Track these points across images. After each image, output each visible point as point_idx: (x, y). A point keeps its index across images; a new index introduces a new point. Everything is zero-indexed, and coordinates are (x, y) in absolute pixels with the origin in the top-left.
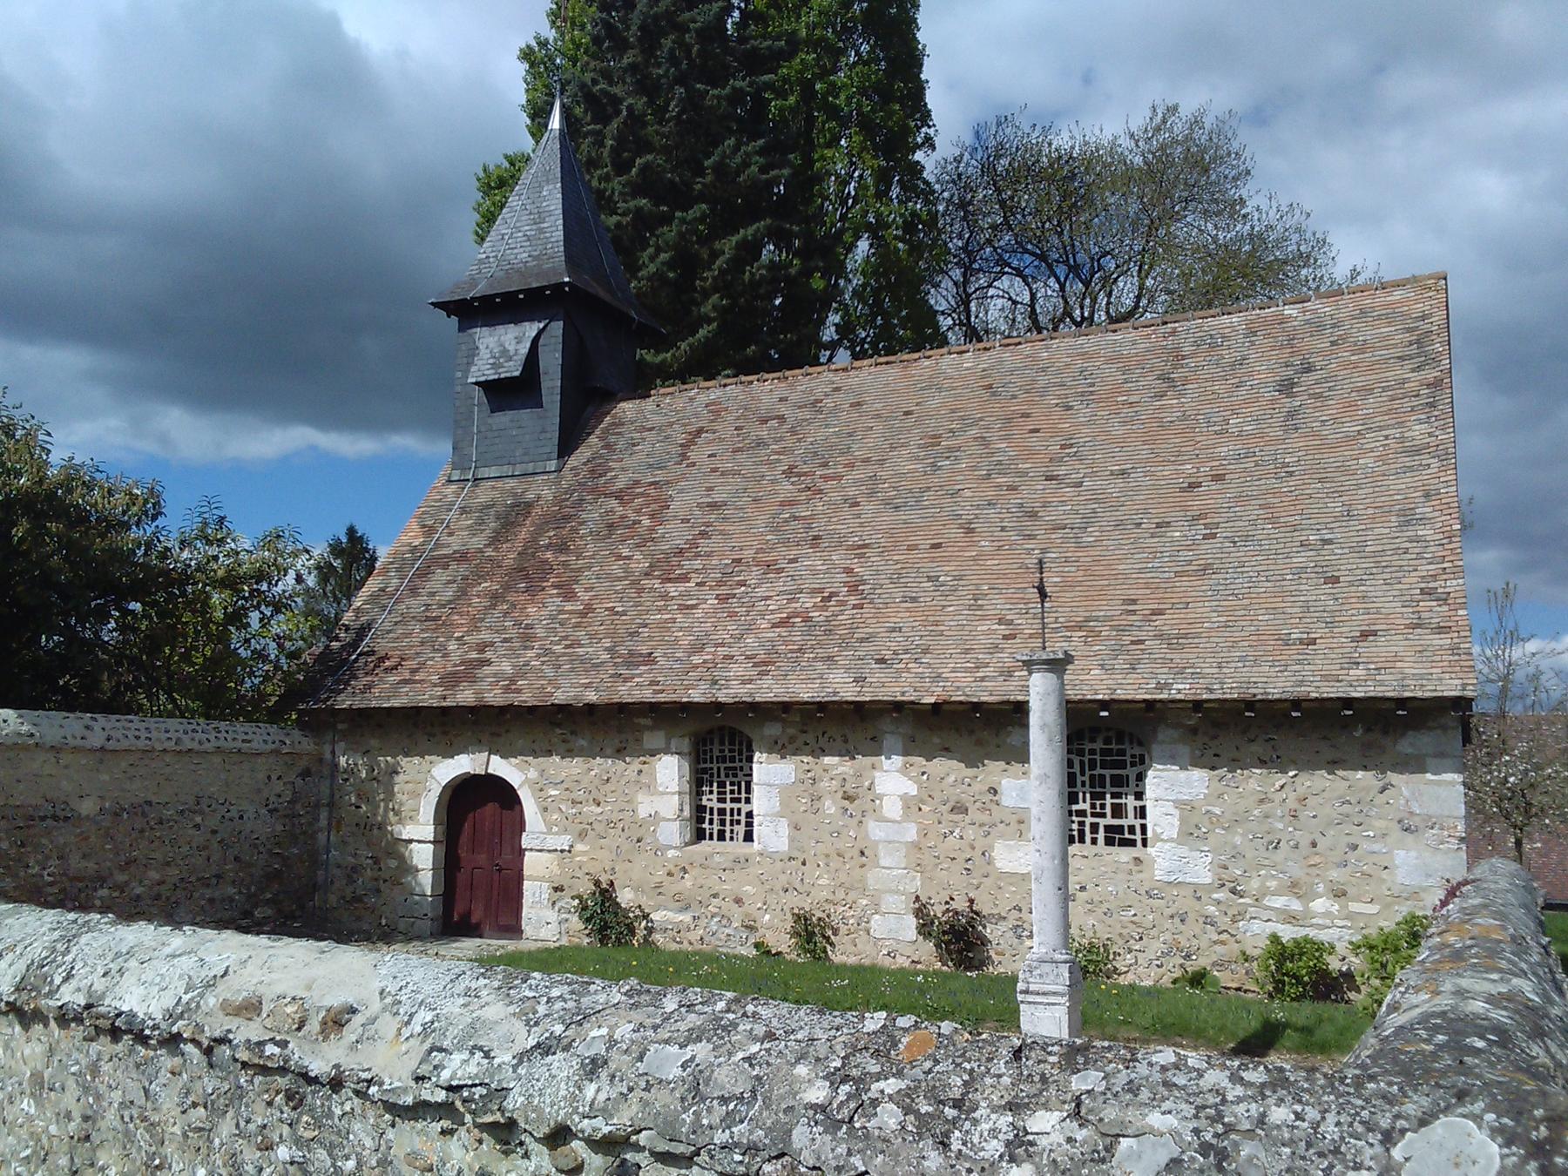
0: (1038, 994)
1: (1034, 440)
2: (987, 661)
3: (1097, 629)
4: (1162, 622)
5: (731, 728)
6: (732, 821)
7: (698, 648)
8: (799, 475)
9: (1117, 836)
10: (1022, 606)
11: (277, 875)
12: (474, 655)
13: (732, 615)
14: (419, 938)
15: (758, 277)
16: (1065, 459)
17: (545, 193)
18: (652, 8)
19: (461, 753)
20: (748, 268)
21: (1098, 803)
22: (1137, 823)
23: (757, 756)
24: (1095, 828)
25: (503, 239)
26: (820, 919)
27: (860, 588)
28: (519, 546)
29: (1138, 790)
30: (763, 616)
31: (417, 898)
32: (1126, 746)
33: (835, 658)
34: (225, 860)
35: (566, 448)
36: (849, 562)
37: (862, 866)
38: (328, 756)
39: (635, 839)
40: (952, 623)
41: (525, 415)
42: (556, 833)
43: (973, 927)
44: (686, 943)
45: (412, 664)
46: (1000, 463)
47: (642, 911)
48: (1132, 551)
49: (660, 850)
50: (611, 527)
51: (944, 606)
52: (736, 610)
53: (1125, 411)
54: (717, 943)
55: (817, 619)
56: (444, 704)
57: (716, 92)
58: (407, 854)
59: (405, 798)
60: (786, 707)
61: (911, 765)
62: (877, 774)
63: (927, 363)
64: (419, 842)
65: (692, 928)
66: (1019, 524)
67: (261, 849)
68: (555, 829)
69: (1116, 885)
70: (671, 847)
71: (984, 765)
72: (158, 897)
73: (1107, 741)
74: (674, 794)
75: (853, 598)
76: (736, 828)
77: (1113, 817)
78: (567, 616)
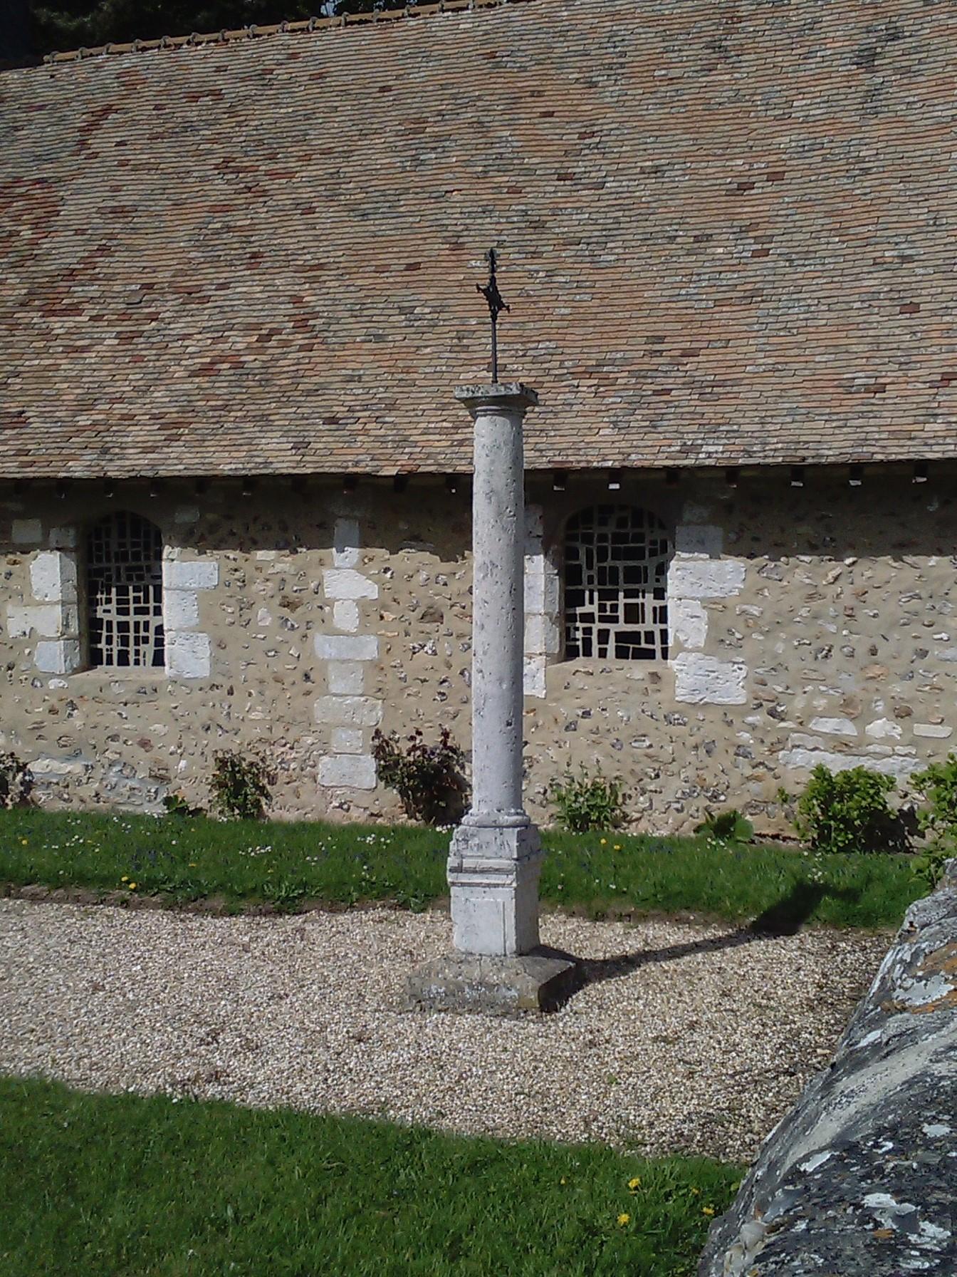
1: (545, 126)
6: (137, 639)
7: (85, 405)
9: (631, 646)
10: (519, 346)
13: (138, 359)
16: (584, 152)
21: (609, 603)
24: (603, 636)
26: (252, 764)
27: (311, 322)
32: (645, 530)
33: (272, 418)
36: (297, 288)
37: (308, 693)
40: (427, 370)
43: (449, 768)
47: (15, 760)
48: (663, 274)
49: (37, 680)
51: (418, 347)
52: (144, 353)
53: (662, 89)
54: (118, 799)
55: (251, 365)
61: (371, 560)
62: (326, 572)
65: (84, 781)
66: (521, 238)
69: (628, 710)
70: (53, 676)
71: (464, 558)
73: (622, 523)
74: (56, 603)
75: (300, 336)
76: (142, 647)
77: (626, 622)
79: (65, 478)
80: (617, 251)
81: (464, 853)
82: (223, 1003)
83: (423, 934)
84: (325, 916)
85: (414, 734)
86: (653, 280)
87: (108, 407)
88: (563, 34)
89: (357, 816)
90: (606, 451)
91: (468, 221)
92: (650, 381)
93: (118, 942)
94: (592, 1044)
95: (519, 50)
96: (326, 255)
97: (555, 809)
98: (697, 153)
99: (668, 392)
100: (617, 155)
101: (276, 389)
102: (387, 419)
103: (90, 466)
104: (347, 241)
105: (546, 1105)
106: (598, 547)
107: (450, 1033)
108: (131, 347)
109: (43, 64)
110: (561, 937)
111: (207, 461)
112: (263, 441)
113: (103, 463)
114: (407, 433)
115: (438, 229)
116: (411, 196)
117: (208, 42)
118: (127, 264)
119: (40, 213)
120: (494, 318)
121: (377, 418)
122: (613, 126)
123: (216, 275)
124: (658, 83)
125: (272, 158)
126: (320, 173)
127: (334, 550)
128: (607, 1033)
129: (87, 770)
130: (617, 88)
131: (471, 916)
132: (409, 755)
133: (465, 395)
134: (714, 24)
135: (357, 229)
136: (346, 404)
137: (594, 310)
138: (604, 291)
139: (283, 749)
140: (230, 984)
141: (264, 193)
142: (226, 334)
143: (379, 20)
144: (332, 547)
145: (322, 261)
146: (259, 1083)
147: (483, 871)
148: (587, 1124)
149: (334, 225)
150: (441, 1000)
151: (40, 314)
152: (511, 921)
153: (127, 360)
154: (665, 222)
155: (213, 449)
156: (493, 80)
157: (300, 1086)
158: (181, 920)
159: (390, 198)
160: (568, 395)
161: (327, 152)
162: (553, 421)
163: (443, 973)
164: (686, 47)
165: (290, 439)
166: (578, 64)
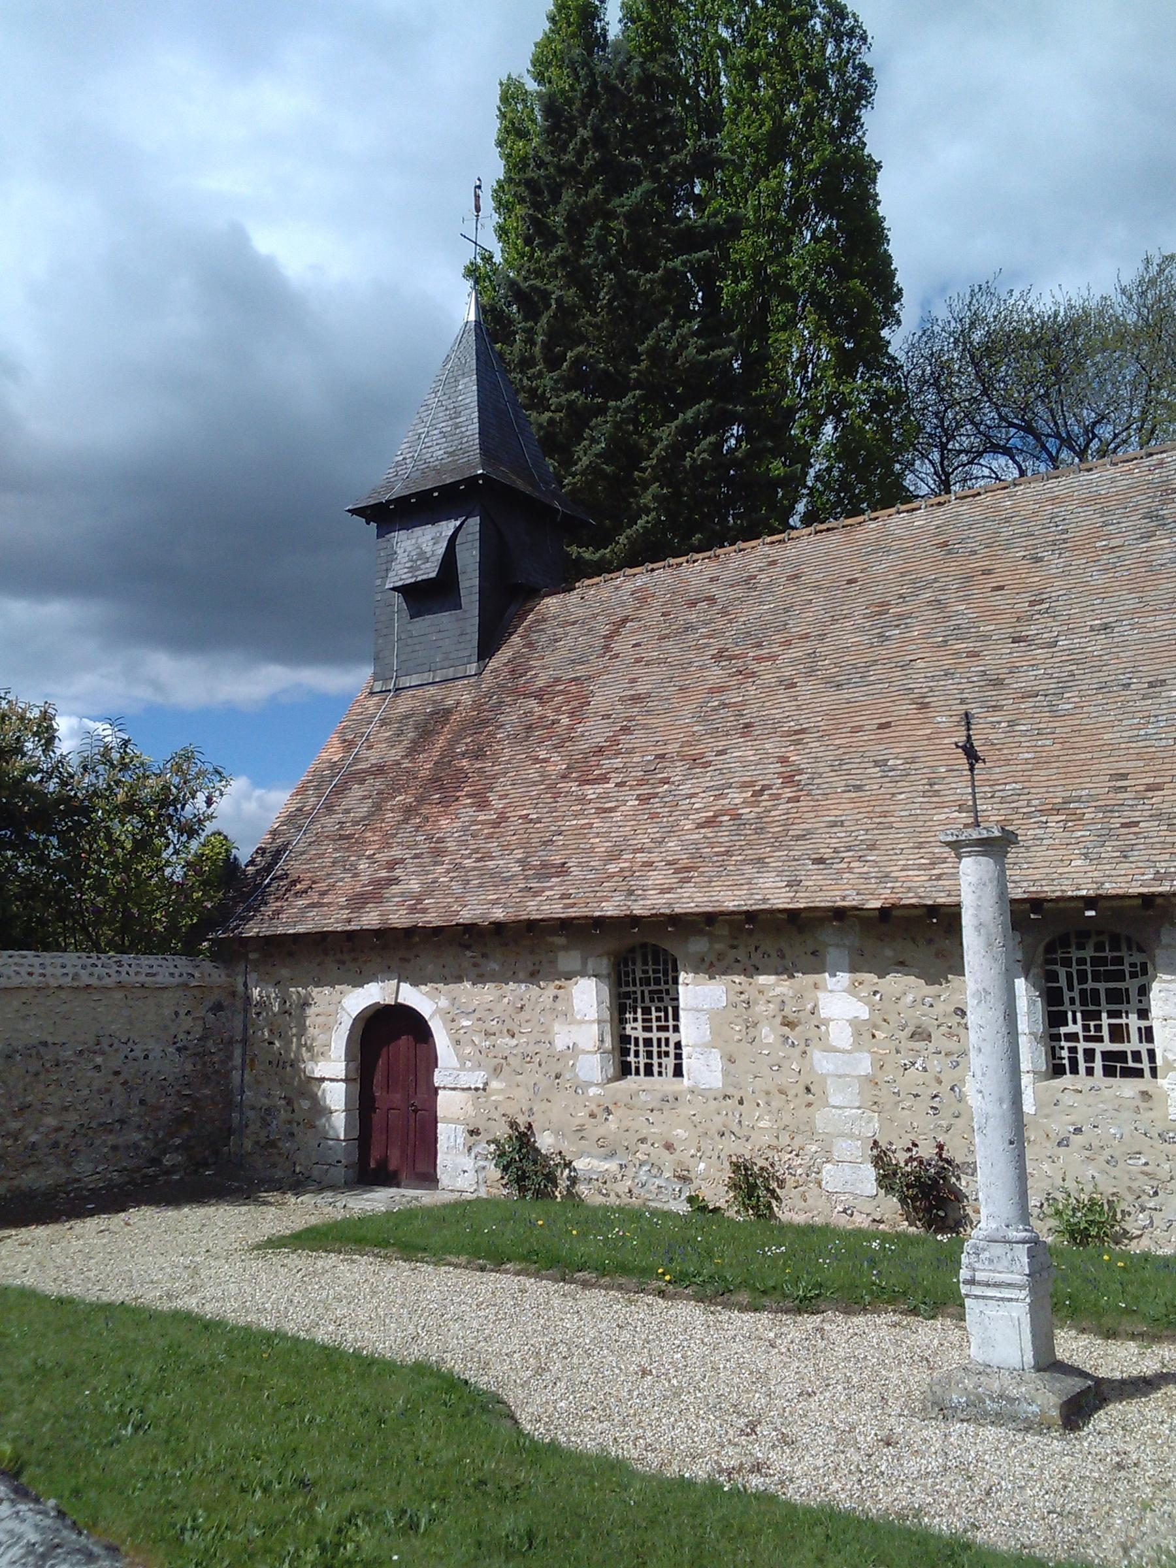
0: (989, 1285)
1: (998, 600)
2: (945, 855)
3: (1078, 811)
4: (1160, 799)
5: (654, 945)
6: (659, 1053)
7: (614, 855)
8: (730, 658)
9: (1119, 1065)
10: (987, 789)
11: (187, 1119)
12: (384, 874)
13: (654, 816)
14: (333, 1187)
17: (460, 387)
18: (580, 198)
19: (371, 981)
20: (688, 454)
21: (1092, 1023)
22: (1143, 1048)
23: (682, 976)
24: (1089, 1055)
25: (419, 438)
26: (762, 1169)
27: (797, 778)
28: (436, 754)
29: (1141, 1006)
31: (331, 1142)
32: (1124, 953)
33: (767, 860)
34: (129, 1103)
35: (486, 650)
36: (783, 750)
37: (809, 1105)
38: (241, 988)
39: (554, 1075)
40: (903, 813)
41: (444, 619)
42: (470, 1069)
43: (944, 1178)
44: (612, 1195)
45: (322, 886)
46: (958, 627)
49: (580, 1087)
50: (529, 728)
51: (893, 794)
52: (659, 810)
53: (1105, 557)
56: (349, 928)
57: (648, 276)
58: (320, 1094)
59: (316, 1031)
60: (710, 918)
61: (860, 984)
62: (821, 995)
63: (873, 525)
64: (332, 1080)
65: (619, 1177)
67: (170, 1090)
68: (469, 1064)
70: (591, 1084)
71: (948, 981)
72: (56, 1145)
73: (1099, 947)
74: (592, 1022)
75: (788, 790)
76: (664, 1060)
77: (1112, 1041)
78: (479, 827)
79: (600, 916)
80: (1073, 700)
81: (977, 1265)
82: (757, 1395)
83: (936, 1342)
84: (840, 1318)
85: (910, 1146)
86: (1111, 724)
87: (631, 856)
89: (861, 1221)
90: (1080, 881)
91: (931, 684)
92: (1117, 814)
93: (659, 1330)
94: (1120, 1466)
95: (969, 538)
96: (807, 721)
97: (1053, 1223)
98: (1143, 610)
99: (1136, 824)
100: (1067, 617)
101: (770, 835)
103: (619, 906)
104: (825, 708)
105: (1079, 1527)
106: (1078, 970)
107: (975, 1444)
108: (649, 806)
109: (575, 589)
110: (1075, 1353)
112: (761, 880)
113: (630, 903)
115: (906, 692)
116: (880, 667)
117: (703, 559)
118: (643, 740)
119: (575, 704)
120: (972, 769)
121: (860, 857)
122: (1061, 593)
123: (715, 744)
124: (1100, 553)
125: (759, 645)
126: (800, 654)
127: (827, 975)
128: (1134, 1457)
129: (621, 1168)
130: (1062, 560)
131: (986, 1329)
132: (906, 1165)
133: (950, 839)
134: (1149, 497)
135: (834, 698)
136: (831, 846)
137: (1056, 753)
138: (1064, 736)
139: (789, 1156)
140: (761, 1378)
141: (753, 674)
142: (726, 791)
143: (843, 527)
144: (824, 972)
145: (804, 726)
146: (798, 1478)
147: (997, 1285)
148: (1126, 1551)
149: (813, 696)
150: (963, 1411)
151: (577, 783)
153: (646, 817)
154: (1119, 671)
155: (719, 889)
156: (946, 565)
157: (836, 1485)
158: (712, 1313)
159: (860, 670)
160: (1038, 831)
161: (806, 637)
162: (1025, 855)
163: (963, 1383)
164: (1124, 520)
165: (784, 878)
166: (1024, 544)
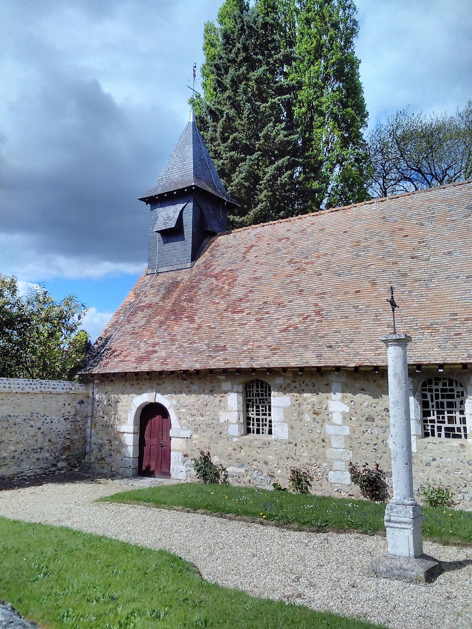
3: (437, 328)
6: (263, 424)
7: (245, 343)
12: (151, 349)
14: (127, 477)
15: (283, 182)
16: (421, 248)
17: (186, 149)
20: (279, 178)
21: (441, 416)
22: (462, 426)
23: (273, 393)
24: (439, 428)
26: (304, 473)
27: (321, 312)
29: (461, 409)
30: (276, 327)
31: (127, 459)
32: (454, 387)
33: (308, 346)
36: (316, 301)
37: (324, 447)
39: (219, 433)
40: (365, 328)
42: (185, 430)
43: (379, 478)
44: (242, 482)
45: (125, 353)
46: (389, 252)
48: (455, 290)
49: (229, 438)
50: (211, 290)
51: (361, 320)
54: (256, 483)
55: (301, 328)
57: (264, 105)
58: (123, 439)
60: (285, 370)
61: (346, 397)
62: (329, 402)
63: (355, 209)
64: (128, 433)
65: (245, 475)
66: (398, 280)
68: (184, 427)
70: (234, 437)
71: (382, 397)
72: (14, 457)
73: (444, 384)
76: (264, 427)
78: (190, 330)
79: (239, 368)
81: (391, 514)
82: (300, 566)
83: (374, 545)
84: (335, 534)
88: (410, 208)
89: (344, 495)
90: (437, 357)
92: (452, 330)
94: (448, 598)
97: (423, 497)
99: (460, 334)
102: (350, 346)
111: (286, 361)
113: (251, 363)
114: (358, 351)
119: (230, 280)
120: (393, 311)
122: (431, 238)
125: (307, 258)
127: (332, 393)
131: (395, 540)
133: (384, 339)
137: (428, 304)
139: (315, 468)
140: (302, 559)
141: (304, 270)
144: (331, 392)
147: (399, 522)
152: (411, 543)
157: (332, 603)
159: (348, 269)
161: (326, 254)
163: (385, 562)
